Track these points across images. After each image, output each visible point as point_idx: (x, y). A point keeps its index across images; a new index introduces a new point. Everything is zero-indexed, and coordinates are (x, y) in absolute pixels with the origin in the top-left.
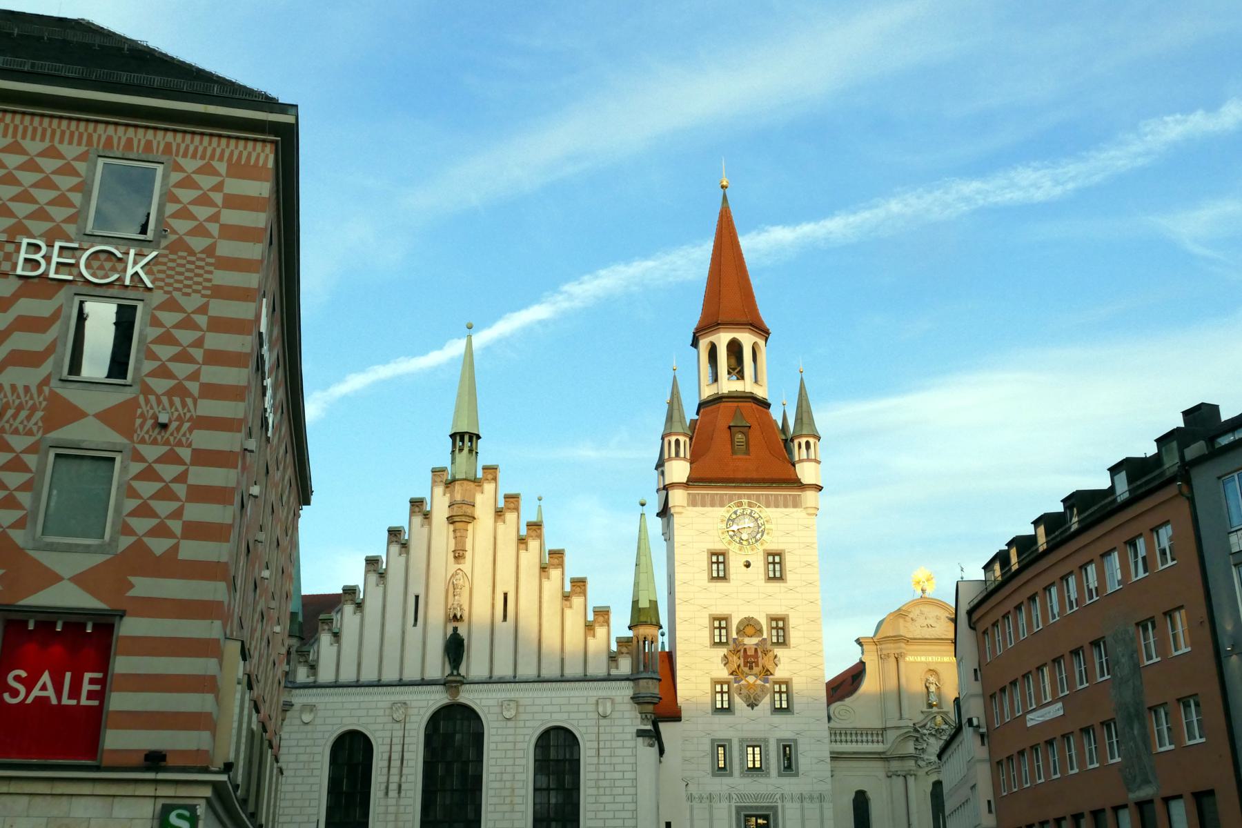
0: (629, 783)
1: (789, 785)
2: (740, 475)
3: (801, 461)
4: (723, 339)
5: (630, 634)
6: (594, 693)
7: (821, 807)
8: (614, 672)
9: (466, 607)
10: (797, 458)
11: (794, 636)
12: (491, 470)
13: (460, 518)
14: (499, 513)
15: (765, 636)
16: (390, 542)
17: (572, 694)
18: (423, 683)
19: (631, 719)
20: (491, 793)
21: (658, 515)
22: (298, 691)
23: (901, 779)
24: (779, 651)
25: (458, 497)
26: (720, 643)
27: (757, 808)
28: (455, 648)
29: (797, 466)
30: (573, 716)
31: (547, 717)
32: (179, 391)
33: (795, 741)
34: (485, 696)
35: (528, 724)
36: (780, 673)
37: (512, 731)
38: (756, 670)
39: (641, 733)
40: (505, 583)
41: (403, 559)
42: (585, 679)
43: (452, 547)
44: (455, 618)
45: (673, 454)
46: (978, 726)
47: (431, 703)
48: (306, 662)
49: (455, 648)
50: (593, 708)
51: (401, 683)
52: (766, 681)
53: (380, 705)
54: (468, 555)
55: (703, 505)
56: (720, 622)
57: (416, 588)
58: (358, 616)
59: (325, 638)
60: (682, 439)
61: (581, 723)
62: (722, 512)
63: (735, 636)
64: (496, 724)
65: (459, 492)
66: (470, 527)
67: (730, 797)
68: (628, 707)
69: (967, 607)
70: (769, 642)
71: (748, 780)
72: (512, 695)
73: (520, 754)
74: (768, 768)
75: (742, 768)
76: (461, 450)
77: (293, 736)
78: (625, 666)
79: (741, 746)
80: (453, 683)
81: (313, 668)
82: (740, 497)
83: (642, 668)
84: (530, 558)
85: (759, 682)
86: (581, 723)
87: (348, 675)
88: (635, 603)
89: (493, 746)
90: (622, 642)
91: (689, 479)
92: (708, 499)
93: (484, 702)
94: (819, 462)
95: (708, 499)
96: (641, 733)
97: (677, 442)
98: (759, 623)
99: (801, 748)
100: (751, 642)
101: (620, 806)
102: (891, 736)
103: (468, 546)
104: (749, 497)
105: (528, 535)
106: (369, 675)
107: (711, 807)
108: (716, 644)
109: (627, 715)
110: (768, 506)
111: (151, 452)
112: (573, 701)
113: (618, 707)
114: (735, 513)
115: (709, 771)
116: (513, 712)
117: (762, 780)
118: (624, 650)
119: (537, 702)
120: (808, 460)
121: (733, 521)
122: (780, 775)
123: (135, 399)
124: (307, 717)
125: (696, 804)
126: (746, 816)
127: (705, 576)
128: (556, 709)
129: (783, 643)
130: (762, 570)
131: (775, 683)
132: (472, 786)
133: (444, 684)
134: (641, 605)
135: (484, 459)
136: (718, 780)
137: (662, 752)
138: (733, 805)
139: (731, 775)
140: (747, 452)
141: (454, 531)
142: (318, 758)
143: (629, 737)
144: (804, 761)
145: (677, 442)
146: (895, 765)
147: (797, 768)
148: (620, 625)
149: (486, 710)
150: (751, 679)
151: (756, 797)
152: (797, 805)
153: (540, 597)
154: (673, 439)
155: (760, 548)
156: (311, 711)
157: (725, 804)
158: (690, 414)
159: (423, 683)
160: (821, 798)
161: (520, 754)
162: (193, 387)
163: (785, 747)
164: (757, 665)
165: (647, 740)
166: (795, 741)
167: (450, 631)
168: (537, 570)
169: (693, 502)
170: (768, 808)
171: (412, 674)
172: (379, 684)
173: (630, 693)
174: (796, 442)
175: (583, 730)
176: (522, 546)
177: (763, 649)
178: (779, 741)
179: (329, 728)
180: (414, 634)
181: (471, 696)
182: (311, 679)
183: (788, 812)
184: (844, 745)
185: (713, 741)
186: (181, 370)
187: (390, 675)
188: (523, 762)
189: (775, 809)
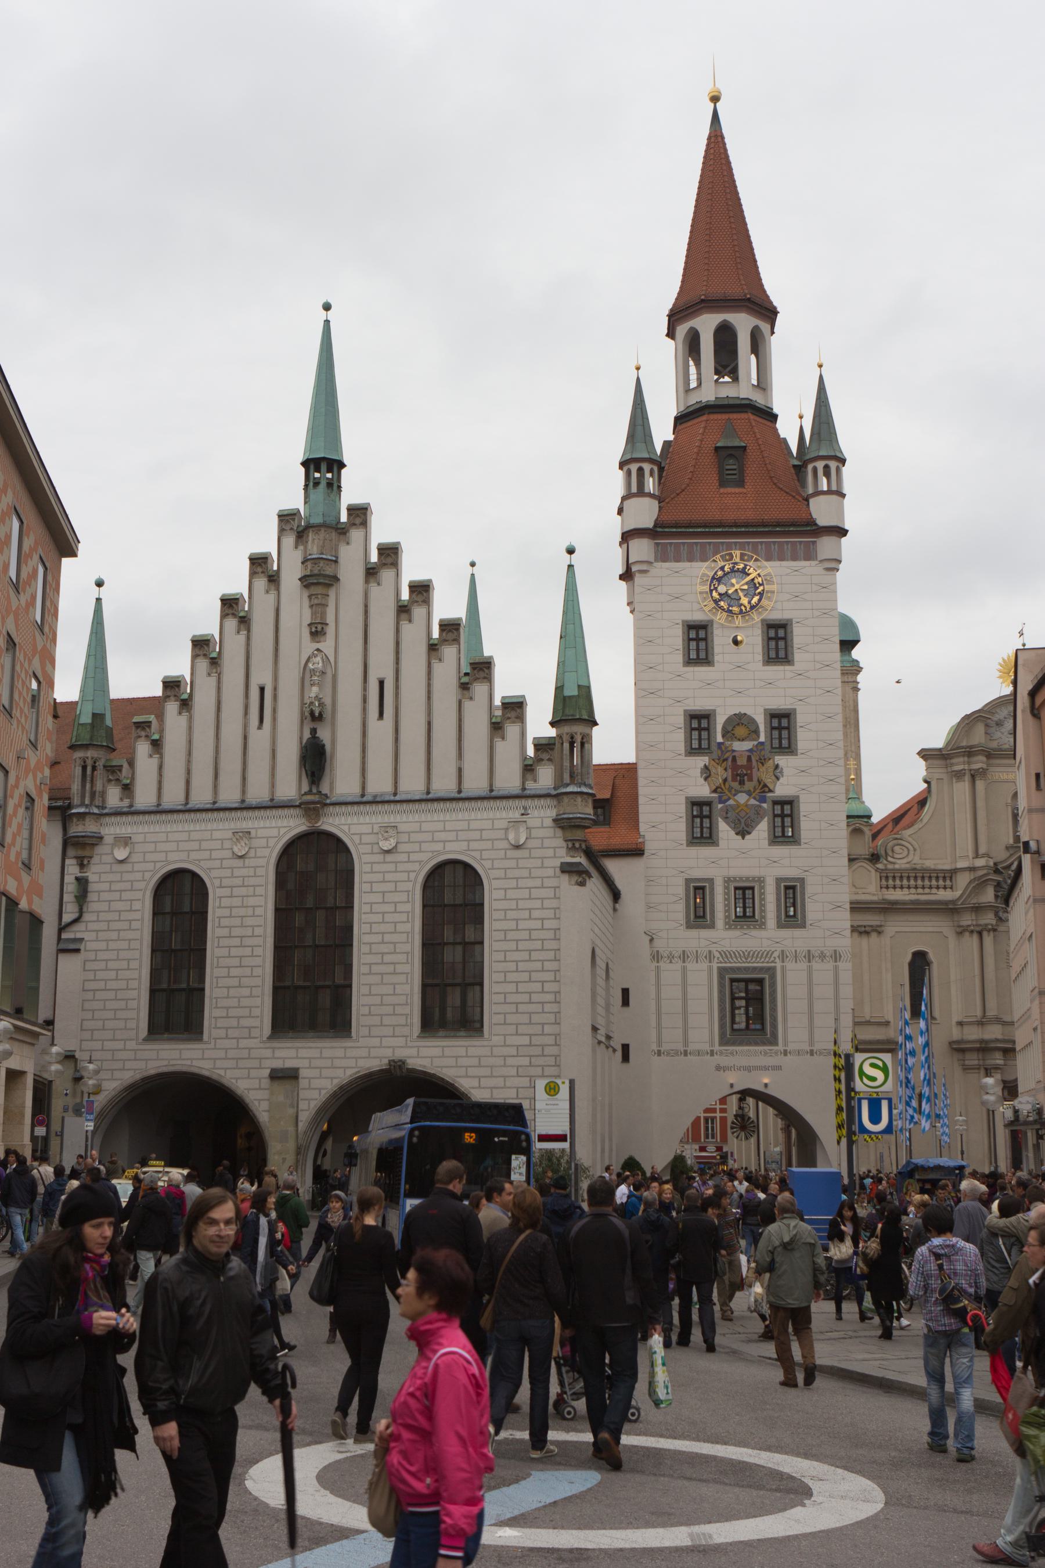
0: (550, 935)
1: (793, 939)
2: (730, 516)
3: (818, 493)
4: (707, 324)
5: (552, 732)
6: (504, 814)
7: (836, 968)
9: (328, 701)
10: (811, 490)
11: (803, 738)
12: (360, 514)
13: (319, 580)
14: (371, 573)
15: (762, 739)
16: (224, 616)
17: (473, 816)
18: (273, 805)
19: (556, 850)
20: (365, 949)
21: (622, 577)
22: (107, 819)
23: (975, 937)
24: (781, 760)
25: (314, 550)
27: (747, 969)
28: (315, 759)
29: (812, 501)
30: (474, 845)
31: (439, 847)
33: (802, 881)
34: (355, 820)
35: (413, 857)
36: (782, 790)
37: (392, 867)
38: (749, 785)
39: (567, 869)
41: (242, 638)
42: (491, 796)
43: (307, 619)
44: (316, 718)
45: (634, 490)
46: (1038, 852)
47: (283, 831)
48: (118, 780)
49: (315, 759)
50: (501, 834)
51: (244, 807)
52: (763, 800)
53: (217, 835)
54: (330, 630)
55: (678, 560)
56: (699, 722)
57: (262, 675)
58: (185, 715)
59: (143, 749)
60: (647, 467)
61: (485, 855)
62: (704, 569)
63: (720, 739)
64: (366, 858)
65: (314, 545)
66: (332, 593)
67: (710, 956)
68: (549, 832)
69: (1030, 687)
70: (768, 747)
71: (737, 933)
72: (392, 819)
74: (764, 917)
75: (726, 917)
76: (317, 484)
77: (104, 877)
78: (546, 777)
79: (726, 888)
80: (314, 805)
81: (127, 789)
82: (729, 547)
83: (567, 778)
84: (414, 636)
85: (753, 802)
86: (485, 855)
87: (174, 796)
88: (559, 689)
89: (366, 887)
90: (543, 746)
91: (656, 524)
92: (684, 551)
93: (354, 829)
94: (843, 496)
95: (684, 551)
97: (640, 470)
98: (752, 721)
99: (809, 890)
100: (742, 747)
101: (538, 965)
102: (962, 881)
103: (330, 618)
104: (742, 547)
105: (412, 601)
106: (201, 796)
107: (684, 970)
108: (692, 751)
109: (547, 843)
110: (768, 559)
112: (474, 825)
113: (535, 833)
114: (722, 569)
115: (683, 922)
116: (392, 842)
117: (754, 933)
118: (545, 756)
119: (425, 827)
120: (829, 492)
121: (719, 580)
122: (780, 926)
124: (121, 854)
125: (664, 965)
126: (732, 980)
127: (679, 658)
128: (452, 836)
129: (788, 748)
130: (759, 649)
131: (775, 803)
132: (340, 943)
133: (299, 806)
134: (567, 692)
135: (349, 496)
136: (694, 933)
137: (616, 895)
138: (715, 966)
139: (712, 926)
140: (741, 483)
141: (310, 597)
142: (137, 905)
143: (551, 872)
144: (813, 910)
145: (640, 470)
146: (967, 920)
147: (804, 917)
148: (539, 723)
149: (356, 838)
150: (742, 798)
151: (747, 955)
152: (803, 965)
153: (429, 685)
154: (634, 467)
155: (756, 617)
156: (126, 844)
157: (704, 965)
158: (662, 431)
159: (273, 805)
160: (836, 956)
161: (403, 897)
163: (787, 888)
164: (751, 779)
165: (575, 878)
166: (802, 881)
167: (307, 735)
168: (423, 648)
169: (662, 556)
170: (761, 969)
171: (258, 792)
172: (214, 809)
173: (552, 813)
174: (810, 467)
175: (488, 864)
176: (404, 616)
177: (759, 756)
178: (779, 881)
179: (150, 866)
180: (259, 739)
181: (337, 821)
183: (790, 977)
184: (899, 892)
185: (688, 881)
187: (229, 795)
188: (407, 907)
189: (771, 971)
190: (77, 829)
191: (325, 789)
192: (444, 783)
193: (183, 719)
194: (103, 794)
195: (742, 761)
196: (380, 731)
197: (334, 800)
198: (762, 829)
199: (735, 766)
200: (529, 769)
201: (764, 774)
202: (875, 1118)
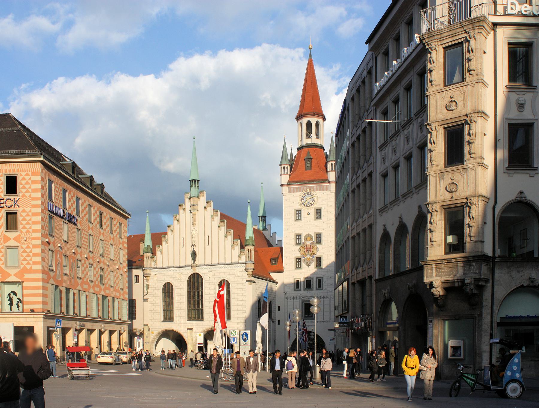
8: (240, 261)
19: (246, 276)
24: (318, 246)
26: (298, 244)
28: (194, 255)
31: (221, 276)
32: (28, 231)
36: (318, 254)
38: (310, 253)
39: (248, 281)
40: (208, 233)
42: (232, 264)
49: (194, 255)
52: (313, 257)
59: (158, 253)
73: (213, 288)
83: (247, 260)
87: (165, 265)
96: (248, 281)
100: (308, 243)
111: (24, 246)
123: (20, 235)
131: (317, 258)
150: (308, 256)
162: (31, 230)
173: (244, 268)
180: (182, 250)
182: (155, 266)
186: (28, 226)
190: (145, 272)
191: (196, 262)
192: (222, 261)
193: (167, 246)
194: (151, 264)
195: (309, 247)
196: (208, 248)
197: (199, 264)
198: (314, 264)
199: (307, 248)
200: (239, 256)
201: (314, 250)
202: (234, 341)
